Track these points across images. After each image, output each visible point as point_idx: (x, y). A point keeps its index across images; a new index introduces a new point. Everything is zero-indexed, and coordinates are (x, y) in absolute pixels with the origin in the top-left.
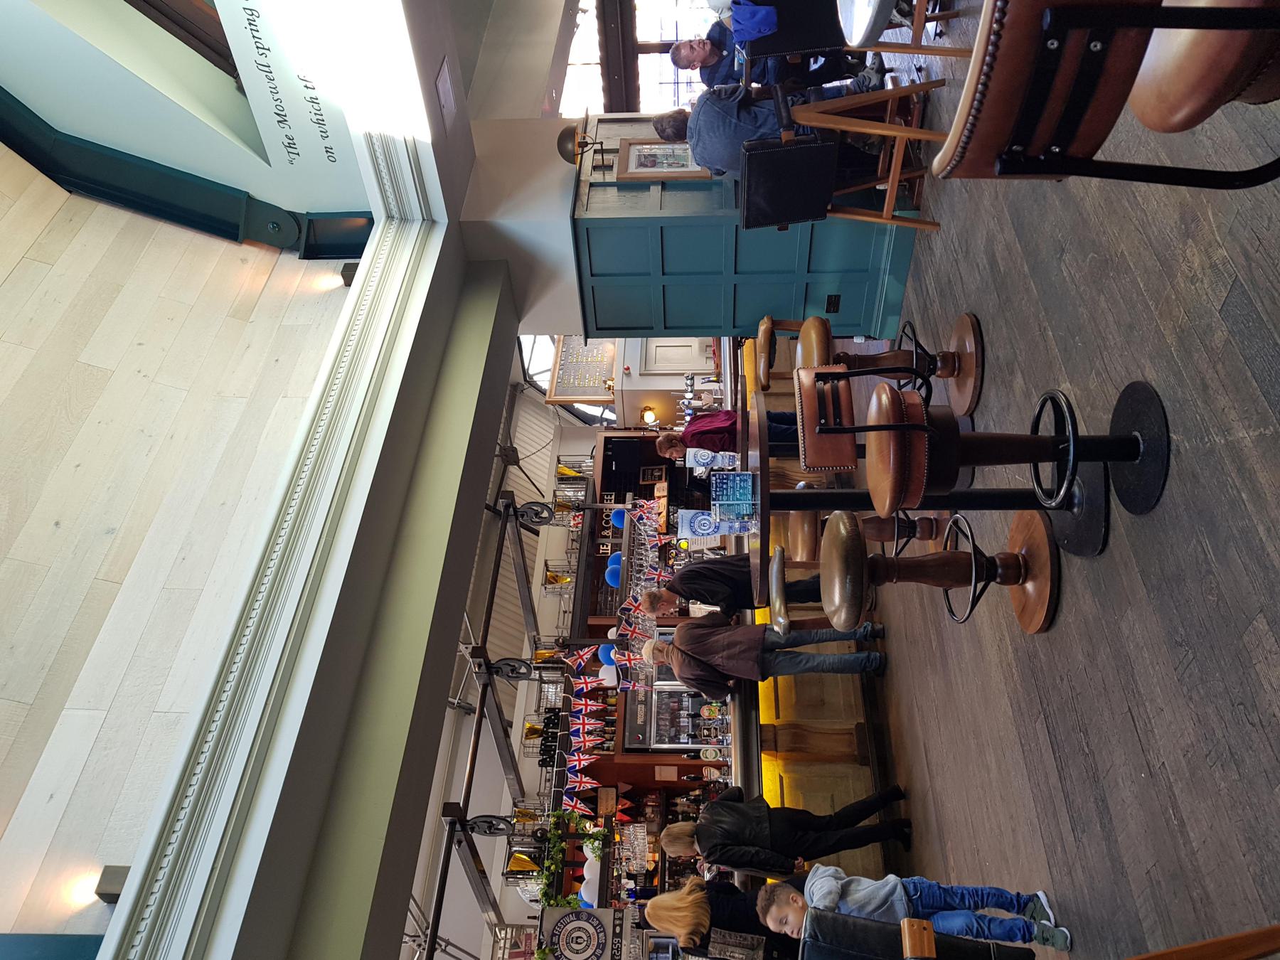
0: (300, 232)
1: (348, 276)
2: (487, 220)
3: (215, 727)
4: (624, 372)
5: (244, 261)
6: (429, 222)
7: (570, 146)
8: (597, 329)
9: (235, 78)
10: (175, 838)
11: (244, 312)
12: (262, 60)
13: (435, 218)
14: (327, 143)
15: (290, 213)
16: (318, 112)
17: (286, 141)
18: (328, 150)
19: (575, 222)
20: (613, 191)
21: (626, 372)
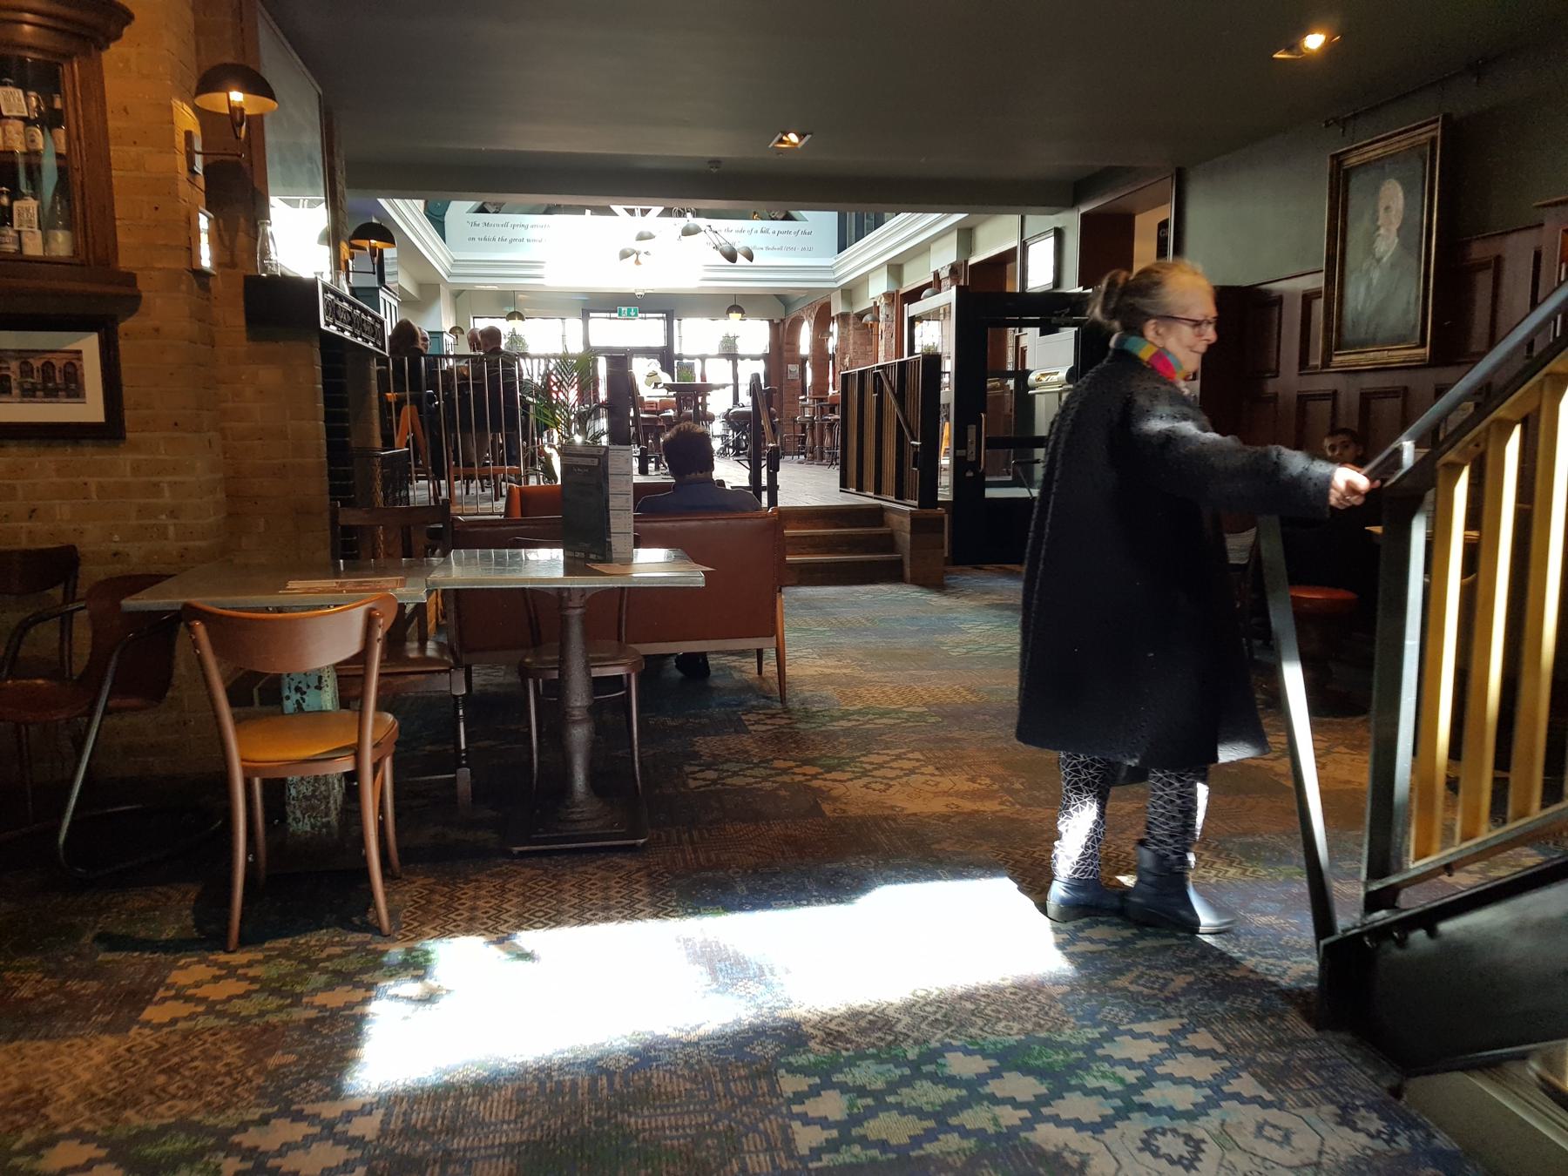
18: (474, 239)
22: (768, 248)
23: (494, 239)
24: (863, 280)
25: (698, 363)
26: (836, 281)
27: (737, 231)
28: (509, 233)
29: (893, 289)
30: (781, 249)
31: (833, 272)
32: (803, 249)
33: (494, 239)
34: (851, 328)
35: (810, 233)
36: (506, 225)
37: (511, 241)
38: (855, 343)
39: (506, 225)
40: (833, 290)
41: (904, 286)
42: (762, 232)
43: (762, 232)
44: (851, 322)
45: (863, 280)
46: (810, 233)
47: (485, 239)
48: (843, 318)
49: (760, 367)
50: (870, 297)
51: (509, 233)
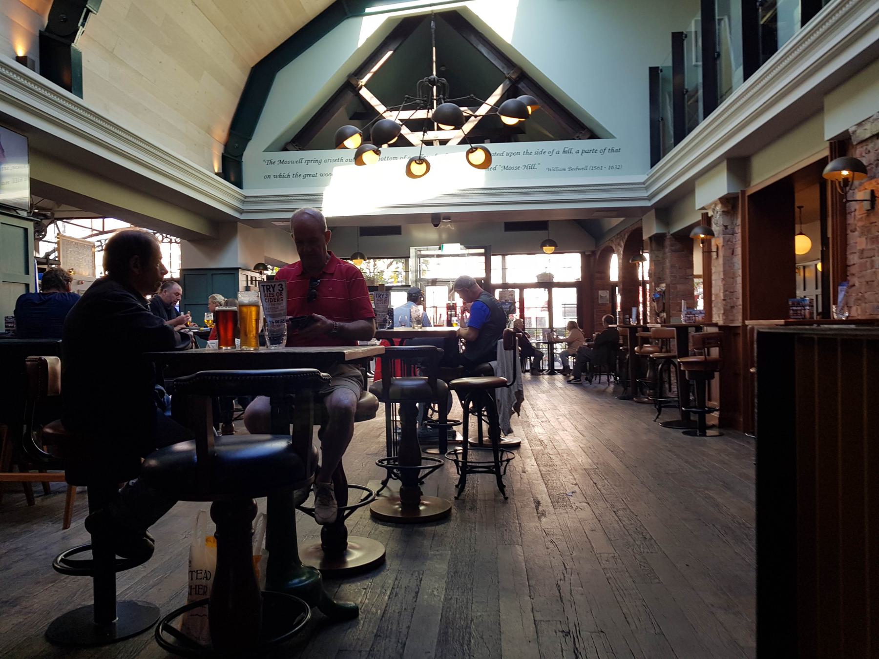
0: (236, 157)
1: (216, 174)
2: (239, 234)
3: (67, 104)
4: (80, 281)
5: (223, 131)
6: (242, 212)
7: (261, 268)
8: (184, 275)
9: (290, 142)
10: (36, 88)
11: (209, 131)
12: (303, 161)
13: (243, 215)
14: (272, 177)
15: (242, 155)
16: (284, 177)
17: (273, 161)
19: (240, 268)
20: (246, 285)
21: (80, 282)
22: (571, 169)
23: (289, 176)
24: (687, 191)
25: (517, 291)
26: (649, 198)
27: (536, 153)
28: (303, 169)
29: (736, 190)
30: (585, 169)
31: (647, 188)
32: (611, 168)
33: (289, 176)
34: (667, 250)
35: (618, 151)
36: (300, 161)
37: (304, 177)
38: (672, 266)
39: (300, 161)
40: (644, 210)
41: (754, 183)
42: (564, 152)
43: (564, 152)
44: (667, 243)
45: (687, 191)
46: (618, 151)
47: (280, 176)
48: (658, 240)
49: (570, 296)
50: (698, 206)
51: (303, 169)
